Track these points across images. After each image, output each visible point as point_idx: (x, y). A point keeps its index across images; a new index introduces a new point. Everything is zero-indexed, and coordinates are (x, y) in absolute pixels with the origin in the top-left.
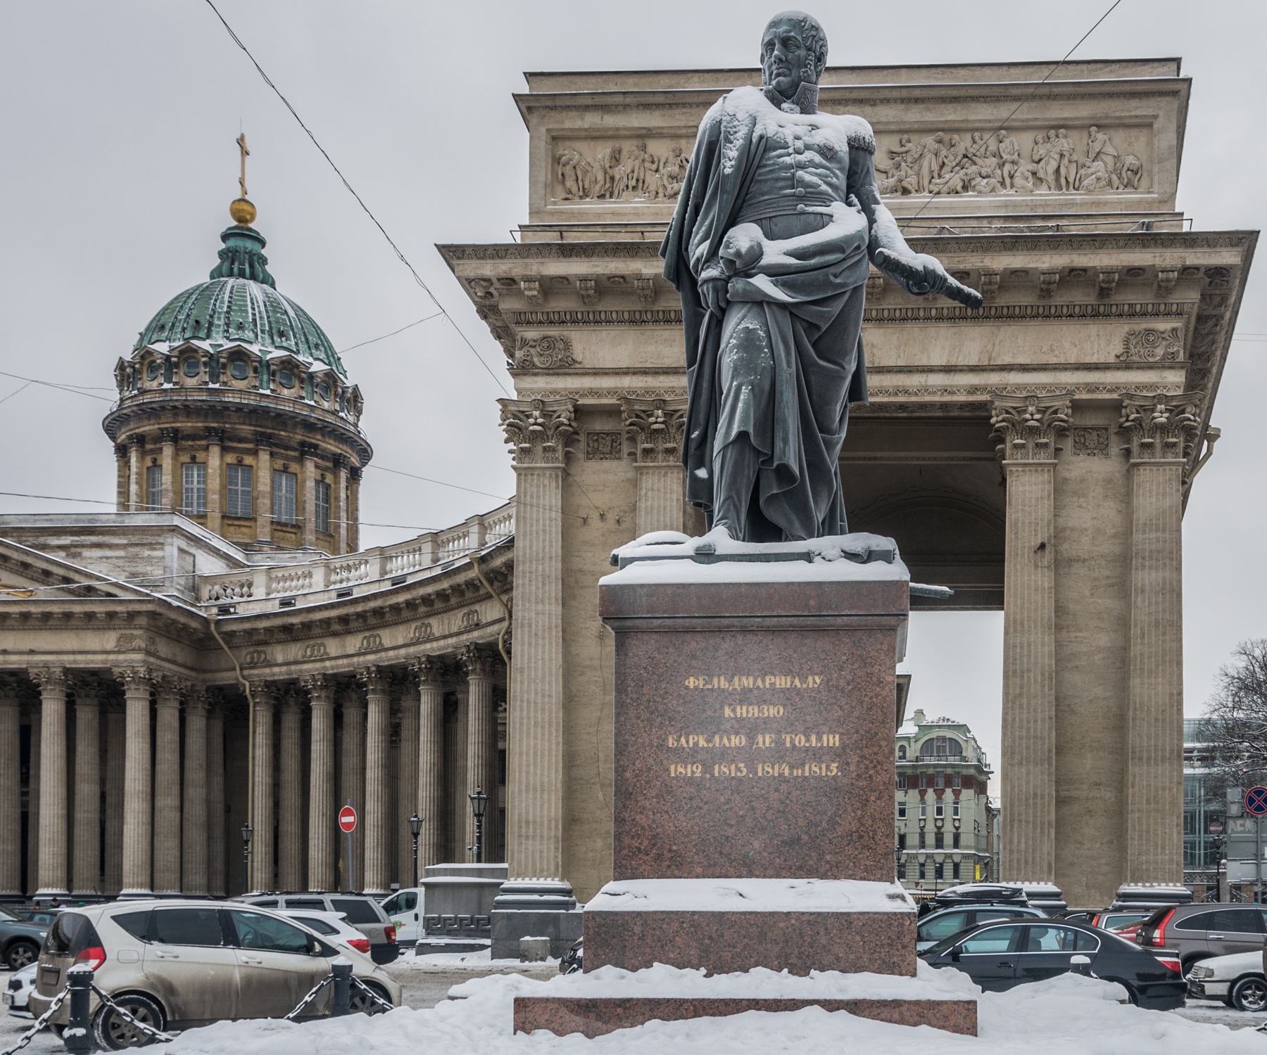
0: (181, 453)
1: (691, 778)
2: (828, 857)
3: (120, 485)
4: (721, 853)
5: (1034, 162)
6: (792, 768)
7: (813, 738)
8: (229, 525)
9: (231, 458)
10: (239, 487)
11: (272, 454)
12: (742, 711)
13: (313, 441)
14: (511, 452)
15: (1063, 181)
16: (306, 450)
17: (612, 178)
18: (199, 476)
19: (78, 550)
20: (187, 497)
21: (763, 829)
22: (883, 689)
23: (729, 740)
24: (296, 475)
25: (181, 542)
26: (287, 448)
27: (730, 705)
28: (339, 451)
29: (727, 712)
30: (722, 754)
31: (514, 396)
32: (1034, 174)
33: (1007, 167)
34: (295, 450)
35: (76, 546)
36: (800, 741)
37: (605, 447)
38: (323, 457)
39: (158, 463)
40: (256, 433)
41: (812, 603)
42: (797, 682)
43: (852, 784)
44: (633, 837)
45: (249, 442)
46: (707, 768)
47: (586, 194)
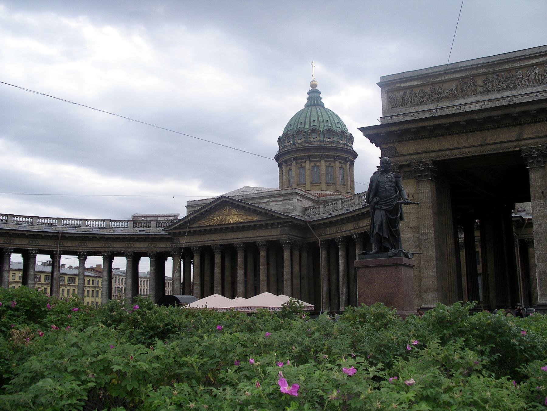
5: (528, 76)
9: (313, 164)
15: (538, 81)
16: (335, 158)
19: (269, 203)
25: (299, 198)
32: (528, 80)
33: (519, 80)
34: (332, 158)
35: (268, 202)
39: (291, 168)
41: (388, 262)
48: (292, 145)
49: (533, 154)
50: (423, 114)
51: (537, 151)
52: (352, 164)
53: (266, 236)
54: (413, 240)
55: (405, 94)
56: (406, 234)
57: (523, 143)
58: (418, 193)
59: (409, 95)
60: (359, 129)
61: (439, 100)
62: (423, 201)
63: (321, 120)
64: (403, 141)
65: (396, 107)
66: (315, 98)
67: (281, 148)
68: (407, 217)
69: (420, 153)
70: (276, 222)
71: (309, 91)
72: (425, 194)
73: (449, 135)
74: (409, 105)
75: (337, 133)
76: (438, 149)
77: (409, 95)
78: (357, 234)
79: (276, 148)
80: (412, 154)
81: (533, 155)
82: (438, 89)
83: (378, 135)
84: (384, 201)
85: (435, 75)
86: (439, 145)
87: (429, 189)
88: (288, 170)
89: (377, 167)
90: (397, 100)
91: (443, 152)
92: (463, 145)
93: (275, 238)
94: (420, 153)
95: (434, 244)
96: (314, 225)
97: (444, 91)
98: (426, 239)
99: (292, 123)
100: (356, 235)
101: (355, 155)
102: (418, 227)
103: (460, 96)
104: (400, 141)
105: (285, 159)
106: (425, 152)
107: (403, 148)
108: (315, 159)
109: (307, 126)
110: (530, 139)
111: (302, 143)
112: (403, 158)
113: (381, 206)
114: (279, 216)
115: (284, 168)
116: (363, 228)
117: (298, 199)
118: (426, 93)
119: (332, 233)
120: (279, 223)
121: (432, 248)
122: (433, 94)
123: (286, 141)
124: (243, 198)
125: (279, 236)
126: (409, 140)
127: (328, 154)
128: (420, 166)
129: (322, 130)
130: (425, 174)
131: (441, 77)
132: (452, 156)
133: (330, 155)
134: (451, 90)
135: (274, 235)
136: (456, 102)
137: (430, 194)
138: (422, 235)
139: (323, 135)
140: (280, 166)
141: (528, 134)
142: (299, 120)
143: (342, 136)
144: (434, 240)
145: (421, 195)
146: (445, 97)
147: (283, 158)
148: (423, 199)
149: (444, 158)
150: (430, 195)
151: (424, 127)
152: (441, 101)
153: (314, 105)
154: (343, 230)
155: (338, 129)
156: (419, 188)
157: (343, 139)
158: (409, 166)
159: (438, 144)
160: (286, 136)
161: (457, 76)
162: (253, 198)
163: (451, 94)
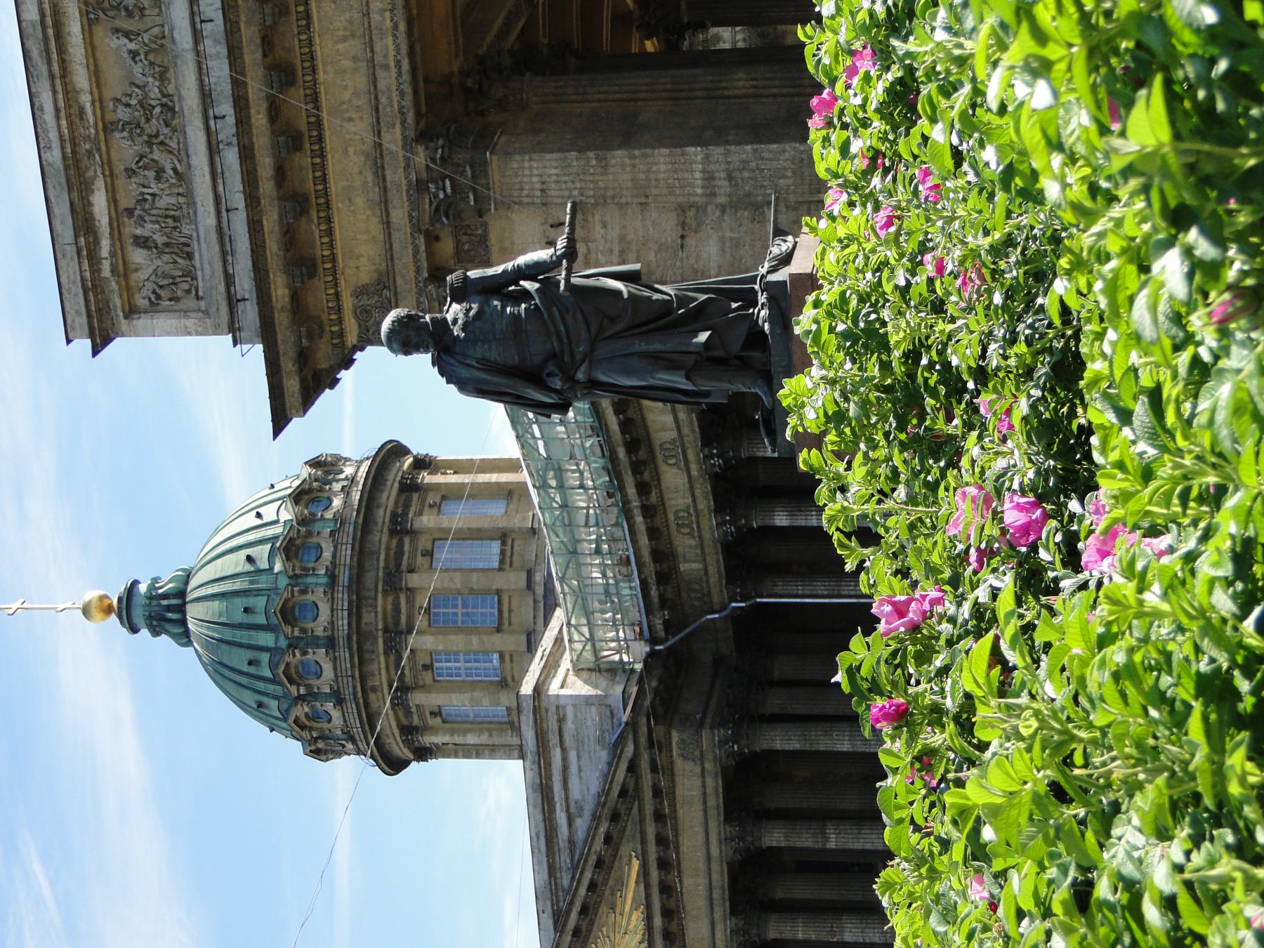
0: (421, 683)
3: (467, 756)
8: (510, 624)
9: (420, 621)
11: (411, 571)
13: (387, 520)
16: (400, 527)
19: (572, 804)
20: (477, 675)
24: (434, 540)
26: (400, 552)
28: (396, 485)
34: (401, 542)
35: (568, 806)
38: (407, 506)
39: (436, 710)
40: (385, 592)
45: (398, 598)
50: (227, 175)
52: (423, 463)
53: (706, 819)
54: (731, 230)
55: (142, 242)
56: (705, 256)
58: (544, 204)
59: (149, 226)
60: (276, 433)
61: (169, 109)
62: (578, 185)
64: (333, 259)
65: (194, 278)
66: (154, 603)
67: (350, 746)
68: (638, 251)
71: (122, 623)
72: (550, 176)
73: (314, 70)
74: (186, 229)
75: (302, 521)
77: (149, 226)
78: (706, 451)
82: (128, 110)
83: (303, 357)
84: (561, 342)
85: (69, 116)
86: (354, 115)
87: (531, 160)
88: (444, 722)
90: (165, 276)
91: (383, 100)
92: (357, 16)
93: (714, 784)
95: (749, 148)
96: (667, 624)
97: (138, 87)
98: (730, 177)
99: (251, 698)
100: (712, 456)
101: (392, 452)
102: (682, 209)
103: (158, 20)
104: (334, 267)
105: (397, 735)
107: (363, 260)
109: (267, 639)
111: (335, 660)
113: (579, 357)
114: (624, 766)
115: (437, 739)
116: (685, 430)
117: (562, 687)
118: (142, 157)
119: (698, 551)
121: (766, 155)
122: (148, 131)
123: (325, 726)
124: (549, 910)
125: (708, 766)
126: (330, 232)
127: (382, 557)
128: (436, 196)
131: (78, 92)
132: (398, 64)
133: (388, 549)
134: (134, 54)
135: (704, 787)
136: (184, 38)
137: (548, 156)
138: (713, 195)
139: (307, 575)
140: (423, 754)
143: (313, 500)
144: (732, 148)
145: (553, 193)
148: (570, 185)
150: (554, 156)
151: (281, 173)
152: (176, 98)
153: (181, 609)
154: (688, 507)
155: (286, 515)
156: (525, 200)
157: (326, 495)
158: (432, 238)
159: (350, 120)
160: (302, 727)
161: (74, 28)
162: (552, 870)
163: (151, 57)
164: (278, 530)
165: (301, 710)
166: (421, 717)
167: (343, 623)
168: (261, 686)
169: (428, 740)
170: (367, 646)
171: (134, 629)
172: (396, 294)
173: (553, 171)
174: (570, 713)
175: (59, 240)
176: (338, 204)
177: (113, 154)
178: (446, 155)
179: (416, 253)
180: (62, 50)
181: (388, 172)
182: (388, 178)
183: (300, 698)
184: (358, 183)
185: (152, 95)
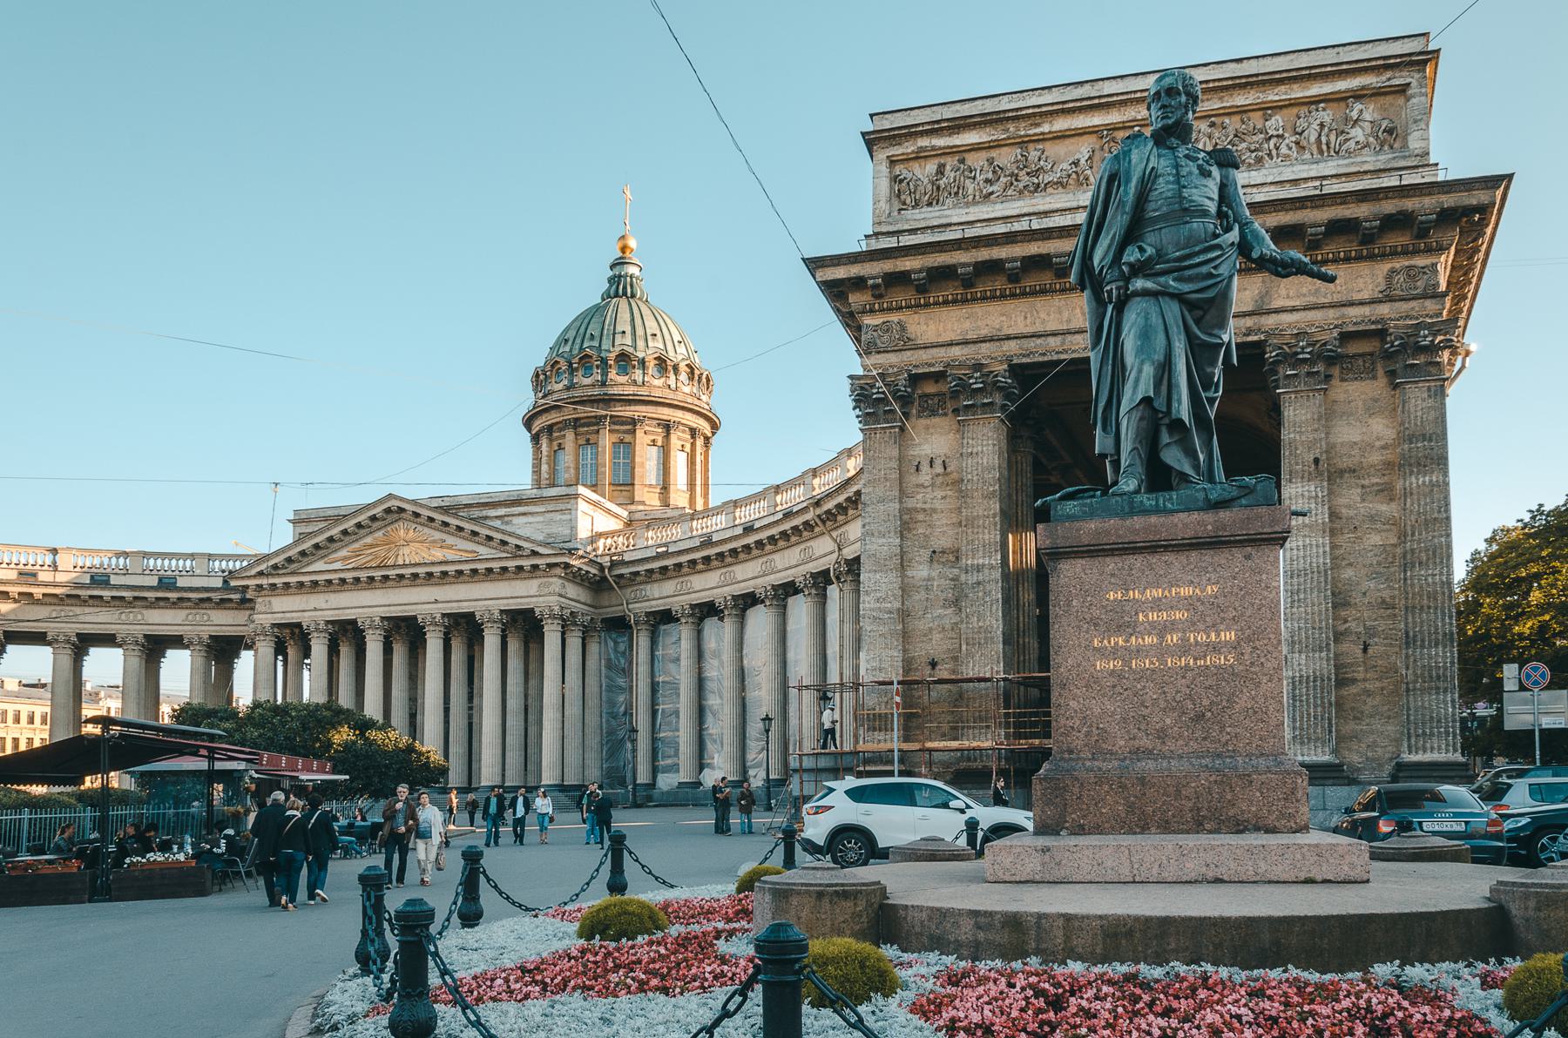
1: (1113, 670)
2: (1228, 730)
4: (1139, 729)
6: (1195, 659)
7: (1213, 635)
10: (621, 461)
12: (1153, 616)
14: (858, 417)
17: (938, 188)
18: (591, 454)
19: (510, 518)
21: (1174, 709)
22: (1271, 592)
23: (1144, 639)
27: (1143, 612)
29: (1141, 617)
30: (1138, 651)
31: (860, 372)
35: (508, 516)
36: (1202, 637)
37: (931, 408)
42: (1197, 591)
43: (1247, 670)
44: (1067, 719)
46: (1126, 663)
47: (916, 205)
48: (568, 388)
49: (1300, 353)
51: (1309, 345)
57: (1270, 321)
63: (640, 332)
67: (541, 395)
69: (975, 342)
70: (526, 563)
76: (1025, 330)
79: (526, 399)
80: (951, 344)
81: (1301, 356)
86: (1029, 321)
87: (994, 445)
88: (555, 451)
89: (851, 377)
91: (1039, 341)
94: (975, 342)
99: (571, 335)
104: (919, 306)
106: (991, 340)
108: (622, 428)
110: (1293, 310)
112: (924, 356)
120: (535, 567)
122: (1021, 174)
123: (553, 380)
128: (970, 378)
129: (641, 355)
130: (985, 401)
132: (1065, 351)
140: (536, 439)
141: (1288, 297)
142: (586, 329)
145: (969, 461)
146: (1057, 183)
147: (544, 419)
149: (1041, 359)
156: (965, 441)
158: (939, 377)
159: (1026, 318)
160: (552, 366)
162: (467, 506)
164: (671, 354)
165: (563, 366)
166: (558, 438)
167: (615, 391)
168: (578, 341)
169: (544, 442)
170: (601, 405)
171: (612, 267)
172: (900, 350)
173: (985, 461)
174: (568, 517)
175: (945, 108)
176: (964, 311)
177: (1005, 149)
178: (1001, 384)
179: (930, 365)
180: (1081, 110)
181: (988, 344)
182: (984, 345)
183: (570, 364)
184: (979, 323)
185: (1046, 176)
